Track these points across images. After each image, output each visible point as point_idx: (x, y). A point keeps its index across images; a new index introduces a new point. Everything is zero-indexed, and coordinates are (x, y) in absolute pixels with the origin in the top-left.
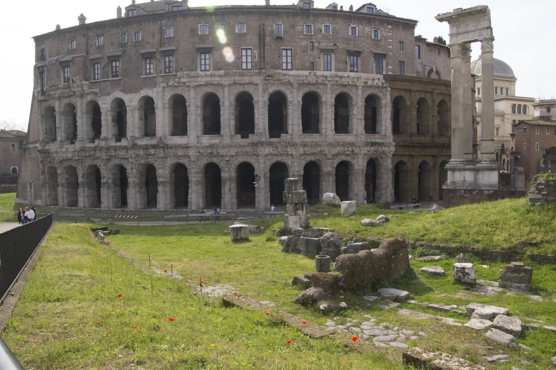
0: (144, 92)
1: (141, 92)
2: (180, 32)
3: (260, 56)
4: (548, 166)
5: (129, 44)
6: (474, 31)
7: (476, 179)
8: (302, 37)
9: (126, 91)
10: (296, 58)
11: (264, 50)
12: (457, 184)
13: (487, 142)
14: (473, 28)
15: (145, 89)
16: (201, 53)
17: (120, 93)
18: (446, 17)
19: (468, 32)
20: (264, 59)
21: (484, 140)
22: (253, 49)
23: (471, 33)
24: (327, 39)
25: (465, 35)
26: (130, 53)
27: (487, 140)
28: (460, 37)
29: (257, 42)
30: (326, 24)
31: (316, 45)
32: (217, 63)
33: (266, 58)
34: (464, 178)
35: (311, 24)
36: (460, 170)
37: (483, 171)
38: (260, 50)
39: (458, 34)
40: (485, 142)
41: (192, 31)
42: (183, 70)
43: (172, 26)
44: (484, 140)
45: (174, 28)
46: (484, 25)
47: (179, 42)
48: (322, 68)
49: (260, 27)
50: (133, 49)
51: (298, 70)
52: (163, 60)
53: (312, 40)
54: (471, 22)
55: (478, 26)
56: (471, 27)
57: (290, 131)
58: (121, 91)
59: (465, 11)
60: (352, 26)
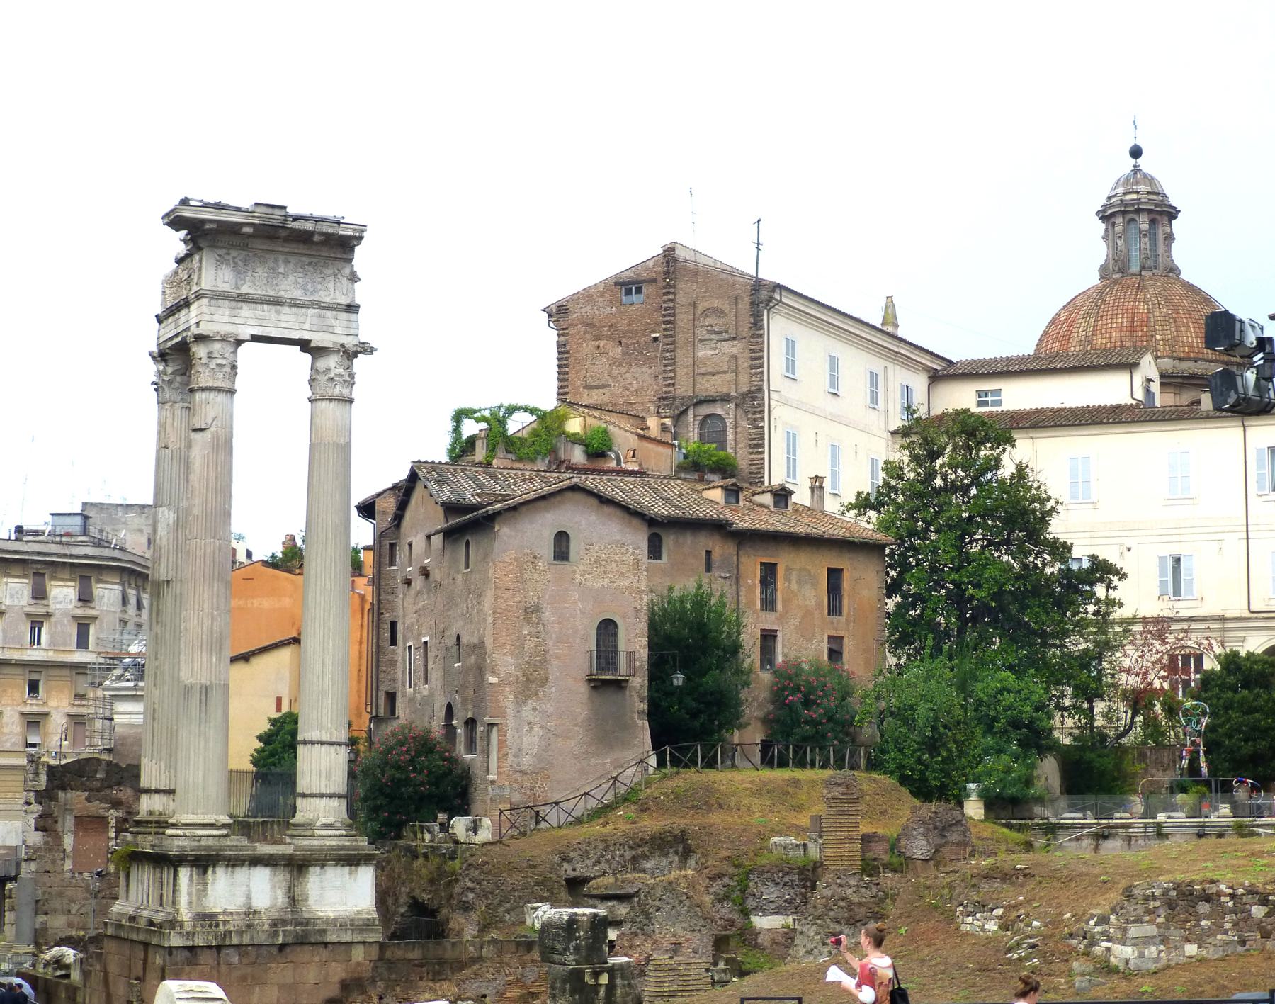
4: (58, 839)
6: (302, 306)
7: (293, 900)
12: (225, 922)
13: (332, 749)
14: (297, 294)
18: (218, 222)
19: (278, 302)
21: (322, 743)
23: (286, 309)
27: (332, 744)
28: (246, 310)
34: (249, 897)
36: (234, 862)
37: (323, 866)
39: (240, 298)
40: (324, 748)
44: (322, 743)
46: (333, 292)
55: (315, 291)
56: (290, 285)
59: (297, 225)
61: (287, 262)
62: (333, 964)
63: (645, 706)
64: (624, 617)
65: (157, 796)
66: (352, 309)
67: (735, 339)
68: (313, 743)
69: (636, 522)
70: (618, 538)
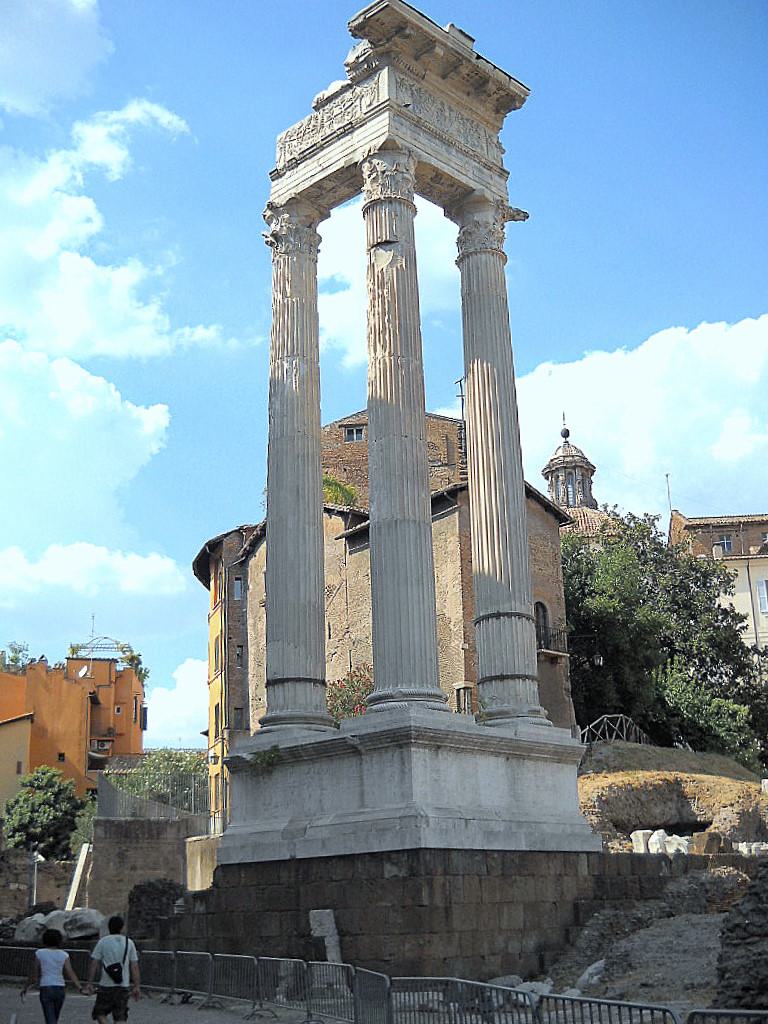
21: (520, 615)
25: (436, 144)
28: (423, 138)
44: (520, 615)
54: (453, 114)
61: (451, 110)
62: (566, 878)
63: (569, 685)
64: (550, 601)
65: (300, 687)
66: (504, 173)
67: (446, 465)
68: (509, 615)
69: (551, 518)
70: (541, 531)
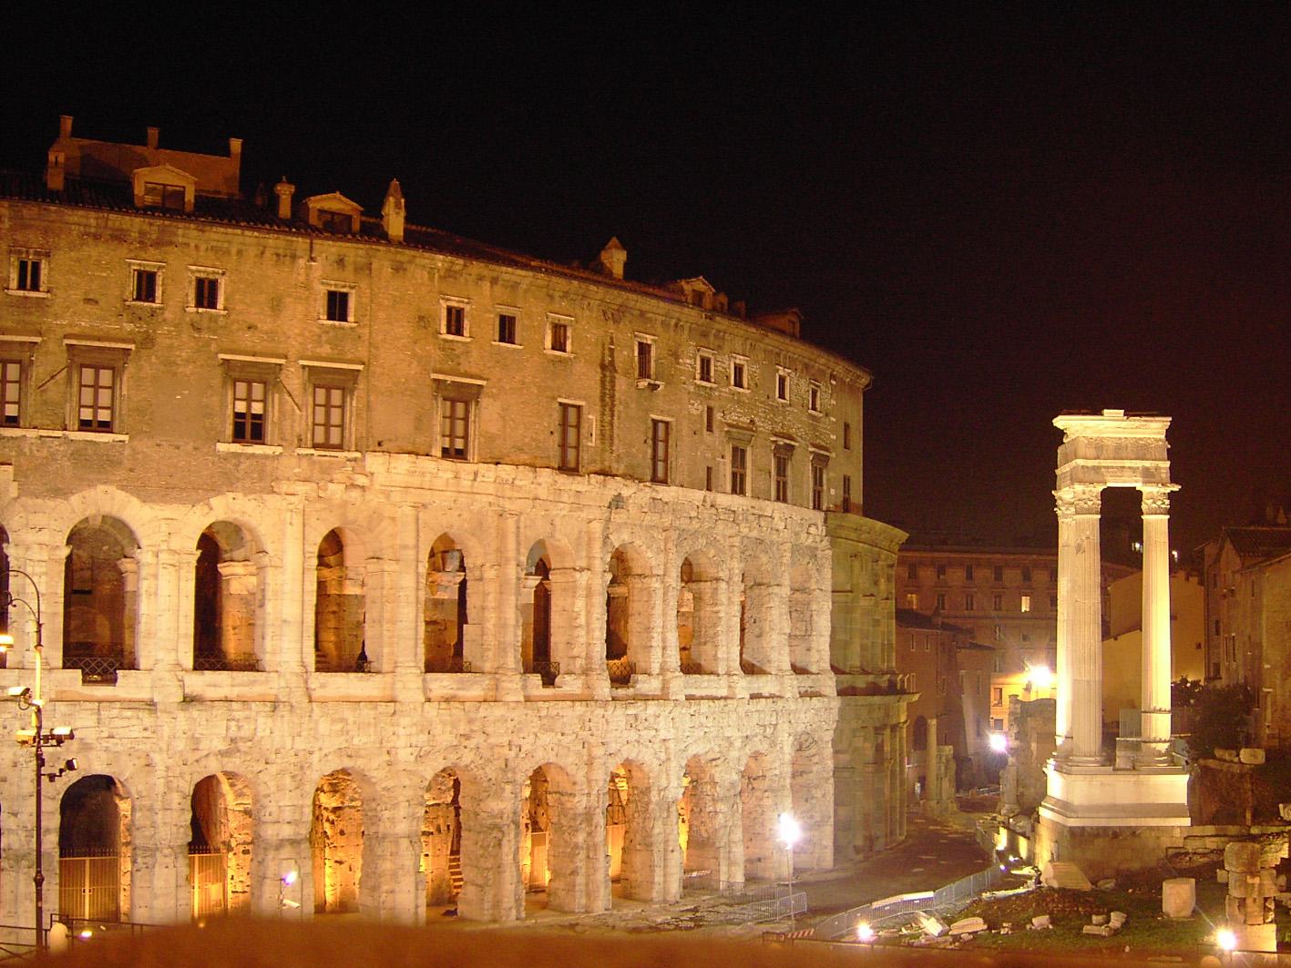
0: (223, 508)
1: (216, 501)
2: (382, 315)
3: (603, 435)
5: (168, 315)
8: (692, 389)
9: (143, 492)
10: (679, 449)
11: (612, 416)
15: (231, 495)
16: (445, 399)
17: (121, 495)
20: (611, 444)
22: (585, 411)
24: (738, 401)
26: (171, 347)
29: (597, 392)
30: (738, 362)
31: (718, 416)
32: (491, 438)
33: (616, 441)
35: (711, 356)
38: (603, 414)
41: (421, 318)
42: (385, 447)
43: (352, 288)
45: (359, 296)
47: (377, 348)
48: (729, 488)
49: (603, 345)
50: (185, 337)
51: (682, 486)
52: (311, 399)
53: (712, 404)
57: (655, 668)
58: (123, 488)
60: (781, 373)
